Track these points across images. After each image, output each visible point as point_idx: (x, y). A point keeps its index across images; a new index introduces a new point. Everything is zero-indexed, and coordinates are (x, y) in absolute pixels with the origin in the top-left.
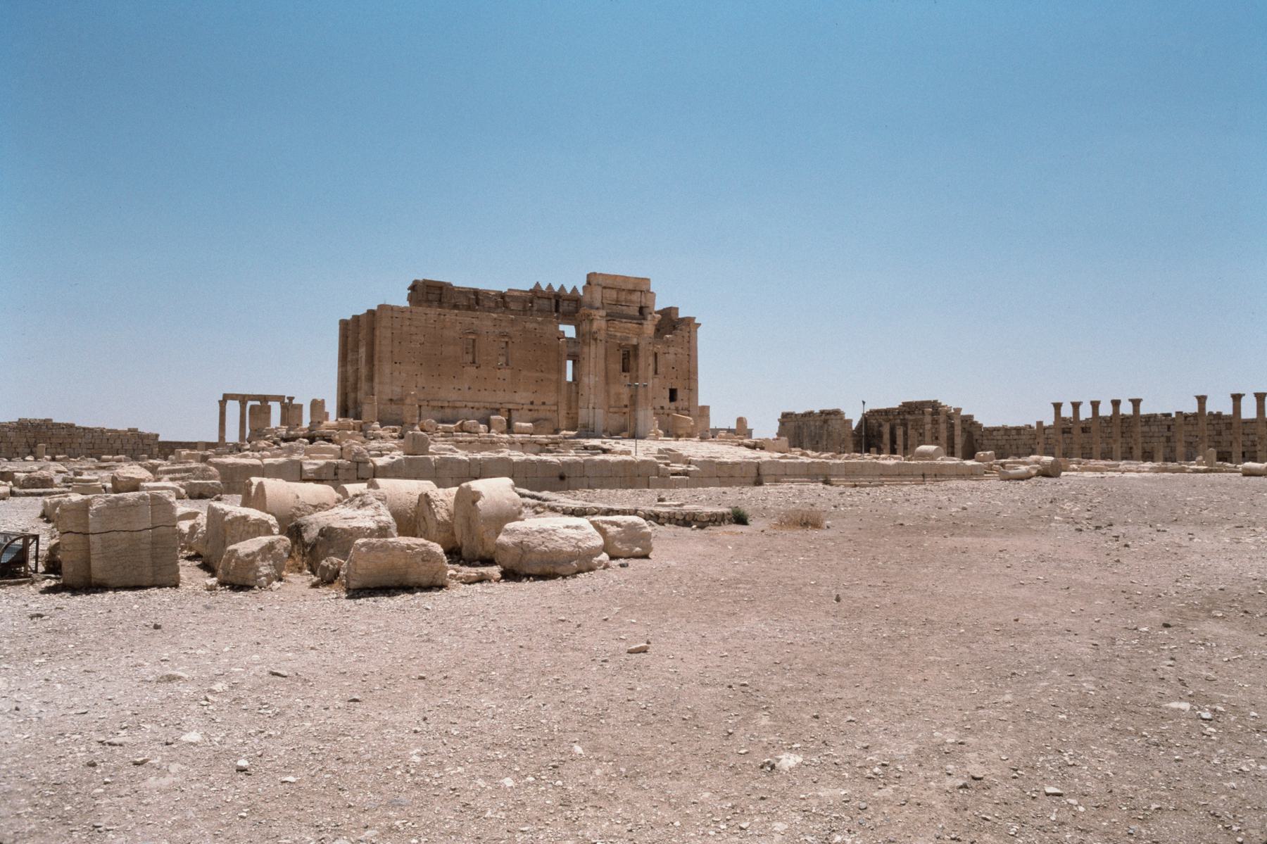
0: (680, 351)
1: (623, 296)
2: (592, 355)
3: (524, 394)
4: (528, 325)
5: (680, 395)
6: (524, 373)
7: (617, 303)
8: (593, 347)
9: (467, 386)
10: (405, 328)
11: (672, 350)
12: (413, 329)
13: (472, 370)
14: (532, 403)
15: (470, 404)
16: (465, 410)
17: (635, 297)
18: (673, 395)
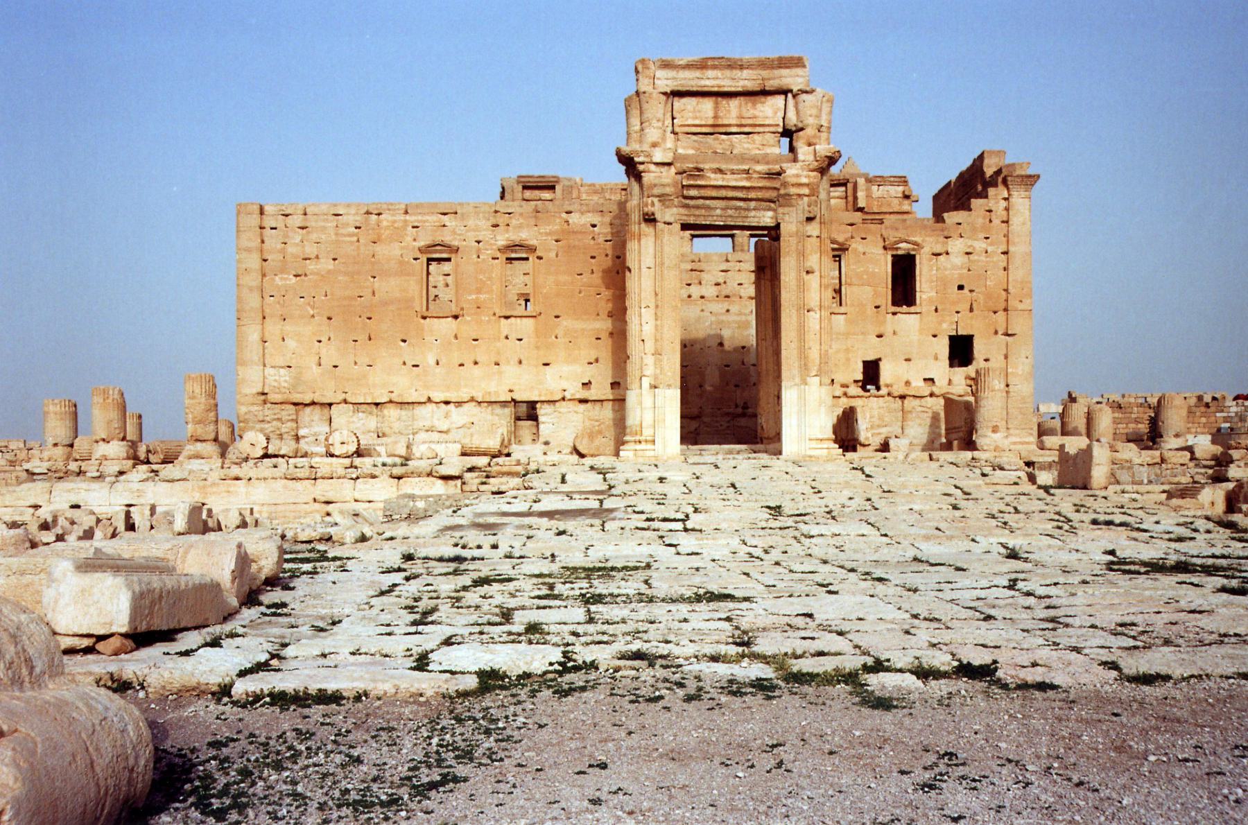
0: (980, 245)
1: (732, 111)
2: (648, 260)
3: (566, 369)
5: (979, 349)
6: (565, 322)
7: (717, 129)
9: (432, 362)
10: (291, 249)
11: (957, 246)
12: (310, 250)
14: (586, 385)
15: (438, 396)
16: (431, 407)
17: (771, 111)
18: (961, 350)
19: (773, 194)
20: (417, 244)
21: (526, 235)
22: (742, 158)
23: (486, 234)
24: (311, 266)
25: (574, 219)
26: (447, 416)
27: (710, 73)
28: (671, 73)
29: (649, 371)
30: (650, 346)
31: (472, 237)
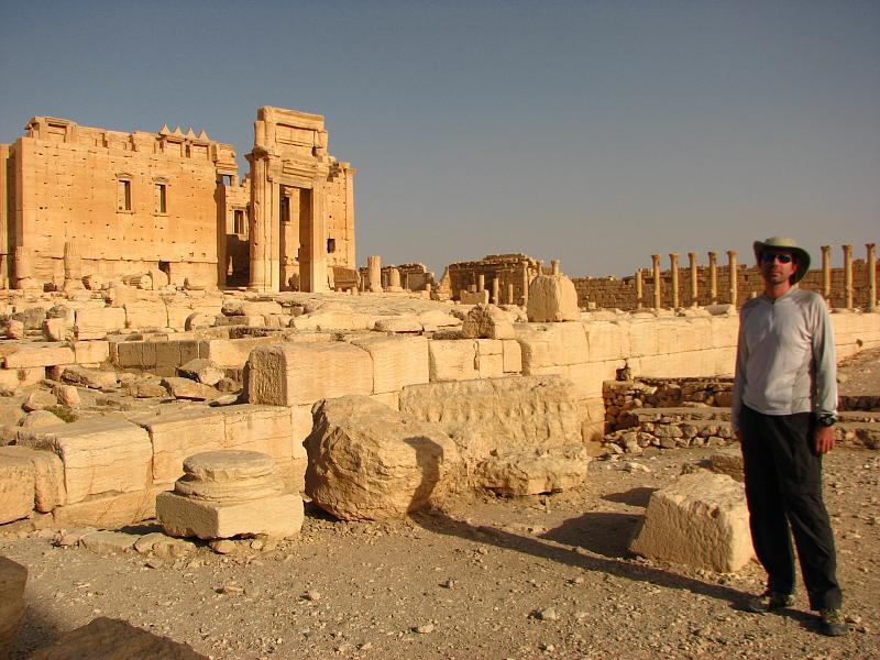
4: (185, 166)
7: (291, 143)
8: (268, 190)
12: (61, 169)
13: (126, 218)
15: (126, 257)
19: (312, 175)
20: (114, 172)
21: (163, 173)
22: (300, 157)
23: (146, 170)
24: (61, 178)
25: (185, 166)
26: (130, 268)
27: (292, 118)
28: (279, 115)
29: (268, 252)
30: (269, 241)
31: (140, 170)
